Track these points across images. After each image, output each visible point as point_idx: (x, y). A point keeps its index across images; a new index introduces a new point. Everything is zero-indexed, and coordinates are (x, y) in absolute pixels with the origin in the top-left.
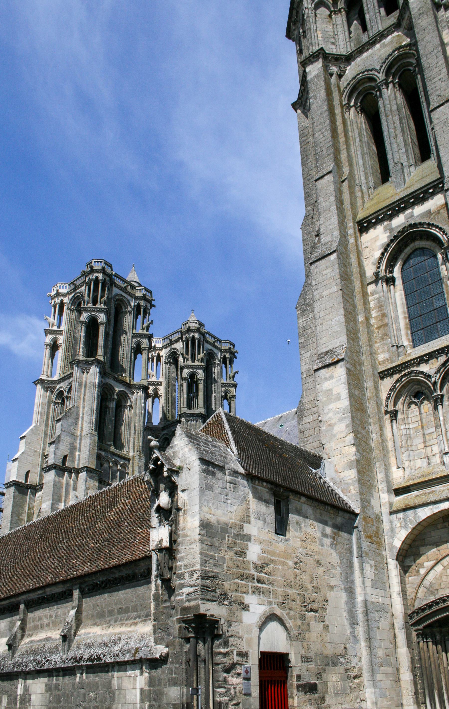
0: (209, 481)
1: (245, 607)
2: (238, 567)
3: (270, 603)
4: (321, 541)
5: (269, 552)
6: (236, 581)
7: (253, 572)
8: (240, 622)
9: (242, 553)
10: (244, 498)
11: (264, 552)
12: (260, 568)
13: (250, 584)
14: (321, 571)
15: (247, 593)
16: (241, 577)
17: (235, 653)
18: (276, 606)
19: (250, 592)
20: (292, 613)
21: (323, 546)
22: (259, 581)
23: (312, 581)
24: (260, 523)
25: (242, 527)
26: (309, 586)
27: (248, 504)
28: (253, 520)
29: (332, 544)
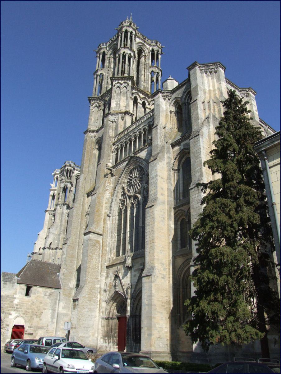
0: (4, 286)
1: (11, 314)
2: (10, 305)
3: (19, 313)
4: (43, 297)
5: (21, 301)
6: (8, 308)
7: (15, 306)
8: (8, 318)
9: (12, 302)
10: (16, 288)
11: (20, 301)
12: (17, 305)
13: (13, 309)
14: (42, 305)
15: (12, 311)
16: (11, 307)
17: (5, 325)
18: (22, 314)
19: (13, 310)
20: (27, 316)
21: (44, 298)
22: (16, 308)
23: (37, 307)
24: (20, 294)
25: (13, 296)
26: (36, 309)
27: (17, 290)
28: (17, 294)
29: (48, 298)
